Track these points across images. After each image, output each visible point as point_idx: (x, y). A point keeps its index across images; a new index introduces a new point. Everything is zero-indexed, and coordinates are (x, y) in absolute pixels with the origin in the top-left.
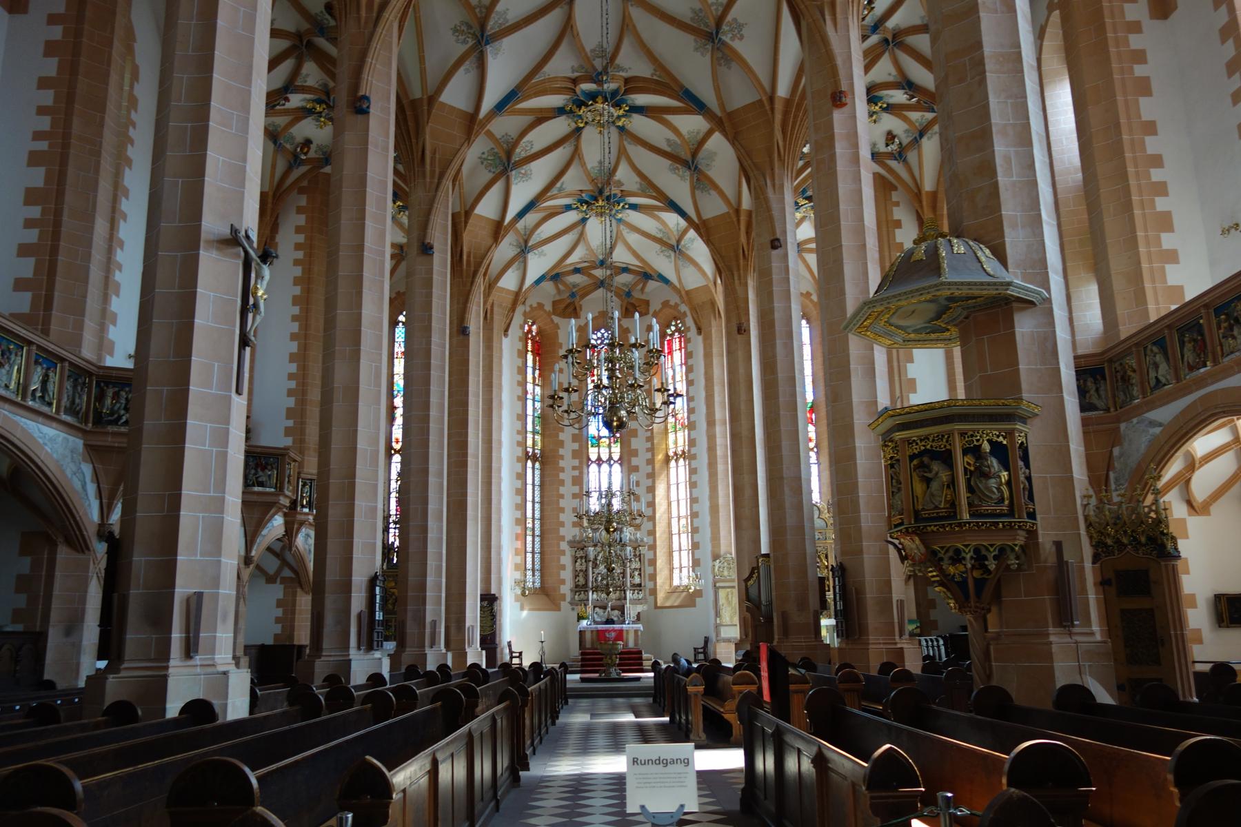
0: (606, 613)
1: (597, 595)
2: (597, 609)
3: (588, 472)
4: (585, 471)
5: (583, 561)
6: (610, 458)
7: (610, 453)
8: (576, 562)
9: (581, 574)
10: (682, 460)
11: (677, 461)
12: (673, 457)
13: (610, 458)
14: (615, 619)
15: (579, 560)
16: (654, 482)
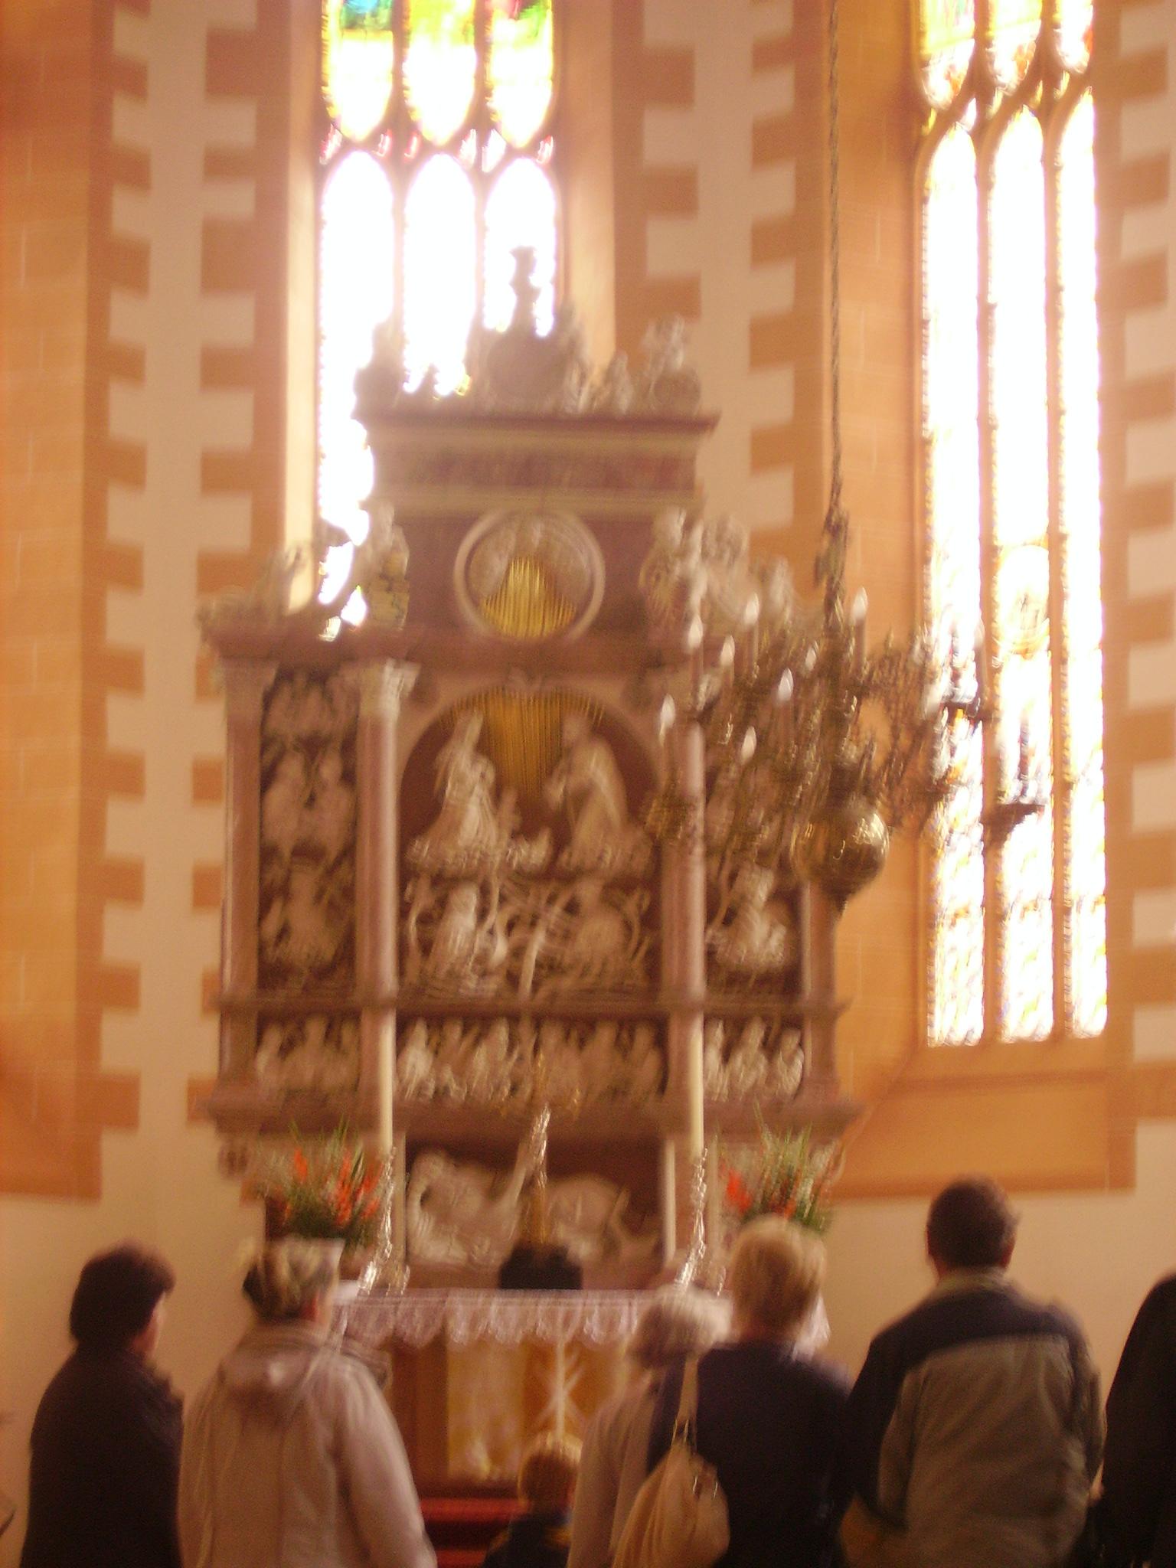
0: (510, 1200)
1: (436, 1050)
2: (435, 1169)
3: (318, 223)
4: (300, 192)
5: (330, 769)
6: (481, 121)
7: (483, 92)
8: (268, 779)
9: (305, 883)
10: (1025, 127)
11: (985, 136)
12: (950, 117)
13: (481, 121)
14: (583, 1249)
15: (292, 769)
16: (807, 287)
